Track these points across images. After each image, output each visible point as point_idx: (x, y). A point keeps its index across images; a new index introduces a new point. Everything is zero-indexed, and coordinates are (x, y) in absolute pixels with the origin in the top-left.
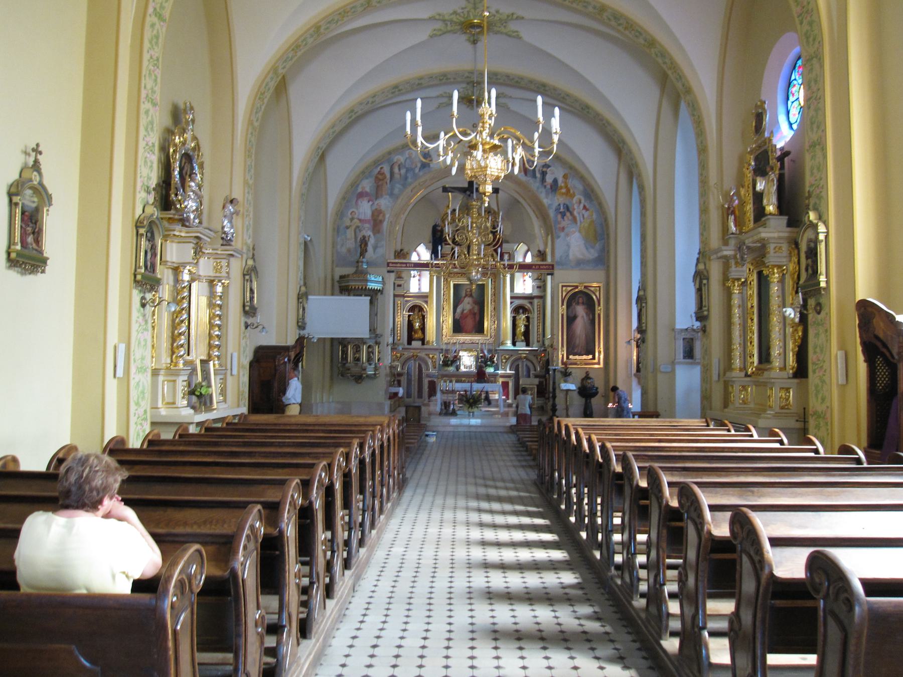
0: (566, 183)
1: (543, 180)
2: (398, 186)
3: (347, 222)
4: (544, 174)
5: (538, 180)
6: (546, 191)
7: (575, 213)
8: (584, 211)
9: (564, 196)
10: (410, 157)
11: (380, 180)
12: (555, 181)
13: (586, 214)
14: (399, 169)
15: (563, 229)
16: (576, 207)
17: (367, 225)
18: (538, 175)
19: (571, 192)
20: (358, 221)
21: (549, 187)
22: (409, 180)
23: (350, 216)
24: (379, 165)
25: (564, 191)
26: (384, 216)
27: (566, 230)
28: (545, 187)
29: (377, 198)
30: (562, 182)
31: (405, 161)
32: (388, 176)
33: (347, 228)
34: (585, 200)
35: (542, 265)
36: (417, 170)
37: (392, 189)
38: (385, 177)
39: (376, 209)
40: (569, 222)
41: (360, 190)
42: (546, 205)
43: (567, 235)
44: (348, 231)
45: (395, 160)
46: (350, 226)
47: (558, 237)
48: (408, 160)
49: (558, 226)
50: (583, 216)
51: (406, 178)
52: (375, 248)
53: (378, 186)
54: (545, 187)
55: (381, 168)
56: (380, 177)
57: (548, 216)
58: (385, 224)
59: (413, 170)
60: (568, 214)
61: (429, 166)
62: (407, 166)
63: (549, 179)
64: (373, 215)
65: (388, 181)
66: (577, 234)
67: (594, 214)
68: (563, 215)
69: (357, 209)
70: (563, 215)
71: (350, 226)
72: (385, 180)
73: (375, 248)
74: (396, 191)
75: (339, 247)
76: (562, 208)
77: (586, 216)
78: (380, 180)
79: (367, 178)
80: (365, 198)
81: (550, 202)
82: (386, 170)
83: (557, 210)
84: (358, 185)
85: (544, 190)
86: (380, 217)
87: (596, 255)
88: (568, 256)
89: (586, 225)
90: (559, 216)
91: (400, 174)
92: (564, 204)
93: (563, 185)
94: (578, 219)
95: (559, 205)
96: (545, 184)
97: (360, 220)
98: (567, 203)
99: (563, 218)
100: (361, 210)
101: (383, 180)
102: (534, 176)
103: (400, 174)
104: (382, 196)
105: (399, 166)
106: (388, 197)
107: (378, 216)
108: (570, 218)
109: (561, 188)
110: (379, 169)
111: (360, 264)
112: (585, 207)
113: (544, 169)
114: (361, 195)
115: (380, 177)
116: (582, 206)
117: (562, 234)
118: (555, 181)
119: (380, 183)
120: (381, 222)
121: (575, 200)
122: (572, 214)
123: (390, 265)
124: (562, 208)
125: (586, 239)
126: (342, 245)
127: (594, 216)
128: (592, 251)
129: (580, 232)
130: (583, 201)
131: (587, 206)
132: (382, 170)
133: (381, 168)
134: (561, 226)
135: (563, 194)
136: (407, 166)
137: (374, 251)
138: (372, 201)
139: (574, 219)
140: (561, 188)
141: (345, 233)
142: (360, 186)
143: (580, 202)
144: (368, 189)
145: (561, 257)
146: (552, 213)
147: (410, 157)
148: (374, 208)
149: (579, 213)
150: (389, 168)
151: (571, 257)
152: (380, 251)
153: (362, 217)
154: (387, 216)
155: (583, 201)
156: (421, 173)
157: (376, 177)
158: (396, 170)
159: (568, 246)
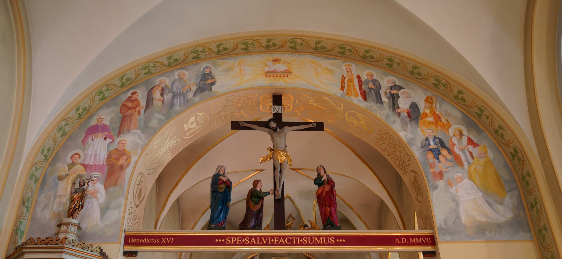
0: (431, 108)
1: (394, 106)
2: (158, 116)
3: (62, 168)
4: (394, 98)
5: (386, 106)
6: (402, 121)
7: (456, 150)
8: (471, 148)
9: (433, 127)
10: (180, 79)
11: (130, 108)
12: (414, 106)
13: (476, 151)
14: (162, 95)
15: (441, 175)
16: (455, 141)
17: (96, 174)
18: (385, 99)
19: (443, 120)
20: (82, 168)
21: (405, 114)
22: (177, 108)
23: (70, 162)
24: (132, 88)
25: (430, 119)
26: (128, 159)
27: (446, 176)
28: (399, 114)
29: (119, 134)
30: (425, 107)
31: (172, 85)
32: (143, 103)
33: (61, 178)
34: (468, 131)
35: (413, 237)
36: (190, 95)
37: (148, 120)
38: (139, 105)
39: (117, 149)
40: (448, 164)
41: (93, 122)
42: (405, 140)
43: (450, 184)
44: (61, 184)
45: (157, 83)
46: (67, 175)
47: (436, 187)
48: (177, 84)
49: (432, 170)
50: (471, 153)
51: (172, 105)
52: (104, 210)
53: (124, 118)
54: (399, 114)
55: (133, 93)
56: (129, 104)
57: (410, 156)
58: (128, 171)
59: (184, 95)
60: (444, 152)
61: (211, 90)
62: (175, 89)
63: (404, 104)
64: (109, 156)
65: (142, 111)
66: (466, 182)
67: (489, 150)
68: (437, 154)
69: (84, 152)
70: (437, 154)
71: (67, 175)
72: (137, 109)
73: (104, 210)
74: (154, 123)
75: (38, 210)
76: (432, 143)
77: (474, 155)
78: (130, 108)
79: (107, 106)
80: (100, 135)
81: (412, 136)
82: (141, 96)
83: (425, 145)
84: (91, 117)
85: (398, 119)
86: (121, 162)
87: (509, 215)
88: (458, 217)
89: (480, 168)
90: (430, 156)
91: (163, 102)
92: (435, 138)
93: (427, 111)
94: (463, 158)
95: (427, 139)
96: (399, 111)
97: (85, 166)
98: (441, 137)
99: (438, 159)
100: (90, 151)
101: (135, 108)
102: (379, 101)
103: (163, 102)
104: (128, 131)
105: (163, 89)
106: (139, 131)
107: (118, 160)
108: (449, 157)
109: (426, 115)
110: (129, 94)
111: (64, 228)
112: (470, 141)
113: (394, 92)
114: (94, 130)
115: (129, 104)
116: (465, 140)
117: (441, 183)
118: (414, 106)
119: (130, 111)
120: (122, 168)
121: (451, 131)
122: (450, 151)
123: (131, 240)
124: (432, 143)
125: (486, 191)
126: (46, 206)
127: (491, 155)
128: (500, 207)
129: (470, 178)
130: (465, 132)
131: (475, 141)
132: (135, 96)
133: (133, 93)
134: (437, 170)
135: (429, 123)
136: (175, 89)
137: (101, 218)
138: (111, 137)
139: (458, 160)
140: (426, 115)
141: (56, 185)
142: (95, 117)
143: (461, 134)
144: (107, 122)
145: (445, 221)
146: (416, 152)
147: (180, 79)
148: (112, 148)
149: (463, 151)
150: (146, 94)
151: (464, 219)
152: (113, 215)
153: (90, 161)
154: (134, 159)
155: (465, 132)
156: (197, 99)
157: (124, 105)
158: (157, 95)
159: (455, 200)
